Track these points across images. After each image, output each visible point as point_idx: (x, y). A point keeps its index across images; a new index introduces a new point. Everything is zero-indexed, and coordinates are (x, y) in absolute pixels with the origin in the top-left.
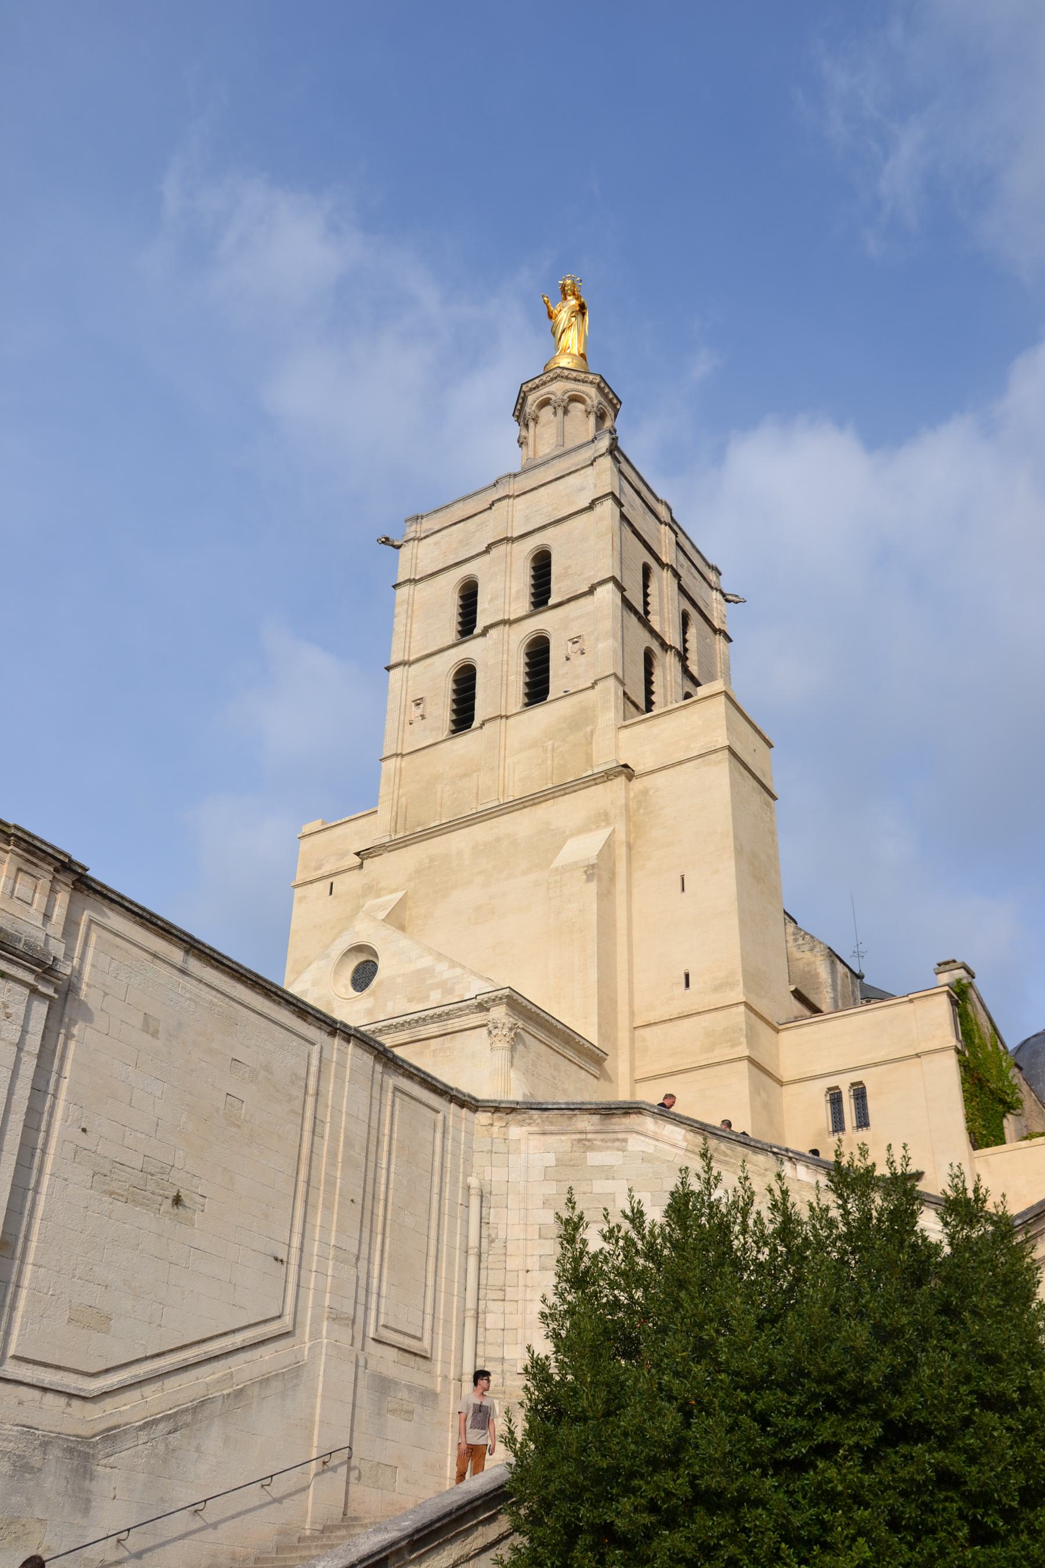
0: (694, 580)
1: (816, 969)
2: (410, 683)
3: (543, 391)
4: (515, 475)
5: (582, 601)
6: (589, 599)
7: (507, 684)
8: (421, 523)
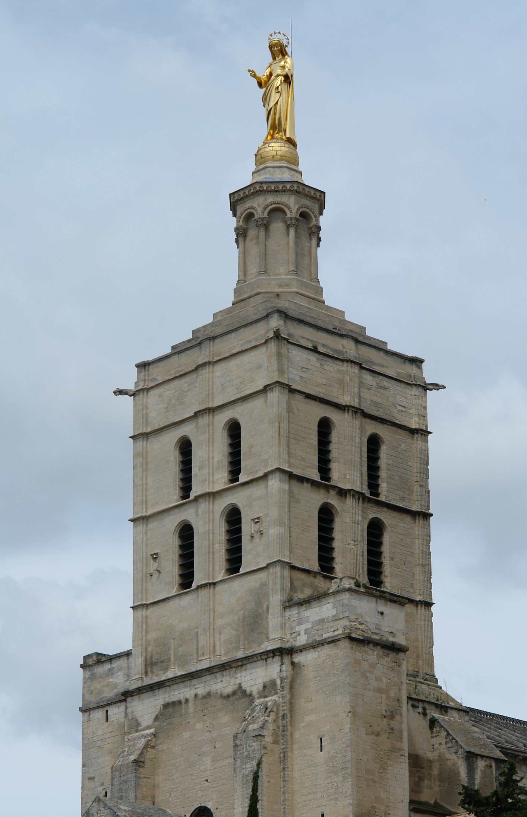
0: (386, 392)
1: (458, 769)
2: (149, 534)
4: (214, 338)
7: (213, 552)
8: (149, 370)
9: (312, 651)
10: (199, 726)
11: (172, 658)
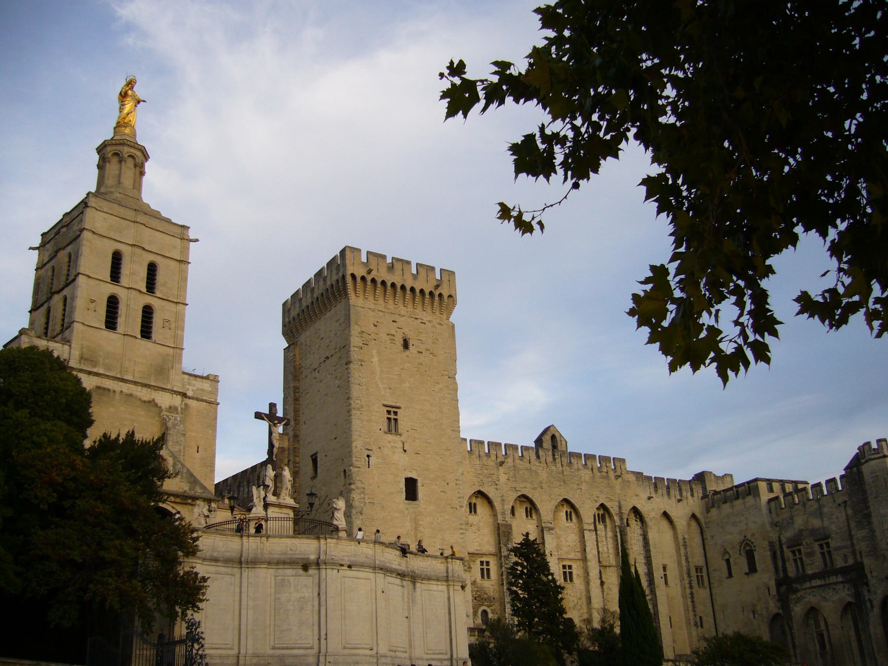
3: (133, 151)
4: (145, 214)
5: (171, 304)
6: (174, 305)
9: (196, 401)
10: (122, 408)
11: (101, 362)
